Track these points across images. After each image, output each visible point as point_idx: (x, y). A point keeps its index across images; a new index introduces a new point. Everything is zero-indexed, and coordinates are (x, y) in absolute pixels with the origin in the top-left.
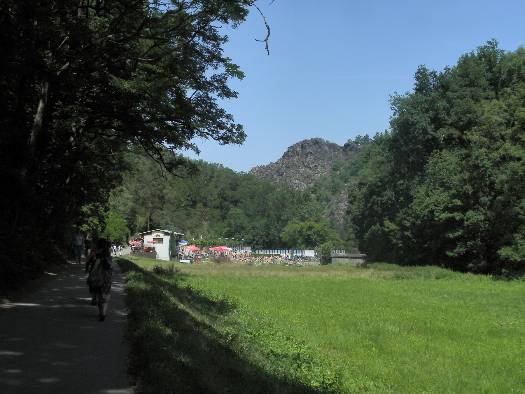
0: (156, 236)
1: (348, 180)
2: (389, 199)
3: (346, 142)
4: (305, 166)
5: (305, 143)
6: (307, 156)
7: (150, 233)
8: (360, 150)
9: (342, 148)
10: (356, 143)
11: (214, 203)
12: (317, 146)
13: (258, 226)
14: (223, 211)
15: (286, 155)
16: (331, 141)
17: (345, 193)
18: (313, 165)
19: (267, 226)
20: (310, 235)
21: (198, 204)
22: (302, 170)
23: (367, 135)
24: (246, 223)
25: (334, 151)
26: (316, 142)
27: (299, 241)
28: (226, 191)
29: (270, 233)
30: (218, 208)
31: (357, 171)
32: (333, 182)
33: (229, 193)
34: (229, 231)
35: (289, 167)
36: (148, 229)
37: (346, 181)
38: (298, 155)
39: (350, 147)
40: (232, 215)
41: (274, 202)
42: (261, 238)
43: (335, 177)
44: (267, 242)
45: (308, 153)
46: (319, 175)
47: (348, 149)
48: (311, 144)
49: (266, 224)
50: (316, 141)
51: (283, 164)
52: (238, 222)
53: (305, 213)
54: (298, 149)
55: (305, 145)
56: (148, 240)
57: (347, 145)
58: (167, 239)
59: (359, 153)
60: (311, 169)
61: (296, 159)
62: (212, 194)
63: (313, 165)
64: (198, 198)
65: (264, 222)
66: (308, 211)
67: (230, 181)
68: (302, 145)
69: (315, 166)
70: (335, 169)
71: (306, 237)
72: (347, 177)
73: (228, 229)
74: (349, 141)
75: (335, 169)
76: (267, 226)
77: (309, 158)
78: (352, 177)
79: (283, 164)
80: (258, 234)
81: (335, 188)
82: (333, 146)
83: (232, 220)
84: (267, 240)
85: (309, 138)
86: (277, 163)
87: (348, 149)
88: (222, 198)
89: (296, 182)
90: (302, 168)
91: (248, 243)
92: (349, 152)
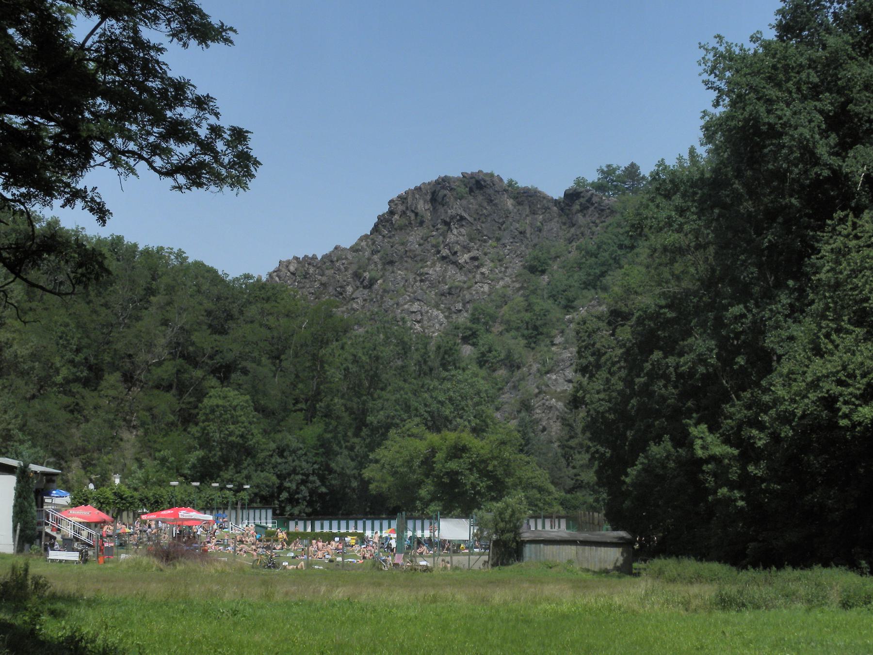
2: (701, 360)
3: (569, 184)
4: (444, 258)
5: (443, 188)
6: (450, 229)
8: (613, 212)
9: (556, 202)
10: (600, 187)
11: (158, 372)
12: (480, 198)
13: (294, 444)
14: (186, 398)
15: (383, 222)
16: (522, 183)
17: (566, 342)
18: (466, 256)
19: (322, 446)
20: (457, 473)
21: (106, 376)
22: (434, 270)
23: (633, 165)
24: (257, 438)
25: (534, 213)
26: (478, 184)
27: (423, 492)
28: (195, 337)
29: (333, 465)
30: (168, 388)
31: (603, 274)
32: (529, 308)
33: (204, 340)
34: (202, 460)
35: (391, 263)
37: (569, 307)
38: (421, 223)
39: (582, 200)
40: (213, 411)
41: (347, 369)
42: (304, 482)
43: (534, 292)
44: (322, 495)
45: (452, 218)
46: (486, 288)
47: (576, 207)
48: (463, 190)
49: (320, 437)
50: (478, 182)
52: (231, 434)
53: (442, 403)
54: (422, 206)
57: (572, 196)
59: (610, 220)
60: (461, 267)
61: (414, 238)
62: (150, 346)
63: (466, 256)
64: (107, 358)
65: (313, 431)
66: (451, 399)
67: (208, 305)
68: (434, 194)
69: (474, 259)
70: (535, 269)
71: (446, 480)
72: (569, 294)
73: (200, 453)
74: (579, 182)
75: (535, 269)
76: (322, 446)
77: (457, 235)
78: (590, 293)
79: (374, 252)
80: (294, 471)
81: (535, 328)
82: (528, 198)
83: (212, 427)
84: (323, 490)
85: (455, 173)
86: (355, 249)
87: (576, 207)
88: (183, 356)
89: (416, 307)
90: (433, 265)
91: (262, 500)
92: (580, 215)
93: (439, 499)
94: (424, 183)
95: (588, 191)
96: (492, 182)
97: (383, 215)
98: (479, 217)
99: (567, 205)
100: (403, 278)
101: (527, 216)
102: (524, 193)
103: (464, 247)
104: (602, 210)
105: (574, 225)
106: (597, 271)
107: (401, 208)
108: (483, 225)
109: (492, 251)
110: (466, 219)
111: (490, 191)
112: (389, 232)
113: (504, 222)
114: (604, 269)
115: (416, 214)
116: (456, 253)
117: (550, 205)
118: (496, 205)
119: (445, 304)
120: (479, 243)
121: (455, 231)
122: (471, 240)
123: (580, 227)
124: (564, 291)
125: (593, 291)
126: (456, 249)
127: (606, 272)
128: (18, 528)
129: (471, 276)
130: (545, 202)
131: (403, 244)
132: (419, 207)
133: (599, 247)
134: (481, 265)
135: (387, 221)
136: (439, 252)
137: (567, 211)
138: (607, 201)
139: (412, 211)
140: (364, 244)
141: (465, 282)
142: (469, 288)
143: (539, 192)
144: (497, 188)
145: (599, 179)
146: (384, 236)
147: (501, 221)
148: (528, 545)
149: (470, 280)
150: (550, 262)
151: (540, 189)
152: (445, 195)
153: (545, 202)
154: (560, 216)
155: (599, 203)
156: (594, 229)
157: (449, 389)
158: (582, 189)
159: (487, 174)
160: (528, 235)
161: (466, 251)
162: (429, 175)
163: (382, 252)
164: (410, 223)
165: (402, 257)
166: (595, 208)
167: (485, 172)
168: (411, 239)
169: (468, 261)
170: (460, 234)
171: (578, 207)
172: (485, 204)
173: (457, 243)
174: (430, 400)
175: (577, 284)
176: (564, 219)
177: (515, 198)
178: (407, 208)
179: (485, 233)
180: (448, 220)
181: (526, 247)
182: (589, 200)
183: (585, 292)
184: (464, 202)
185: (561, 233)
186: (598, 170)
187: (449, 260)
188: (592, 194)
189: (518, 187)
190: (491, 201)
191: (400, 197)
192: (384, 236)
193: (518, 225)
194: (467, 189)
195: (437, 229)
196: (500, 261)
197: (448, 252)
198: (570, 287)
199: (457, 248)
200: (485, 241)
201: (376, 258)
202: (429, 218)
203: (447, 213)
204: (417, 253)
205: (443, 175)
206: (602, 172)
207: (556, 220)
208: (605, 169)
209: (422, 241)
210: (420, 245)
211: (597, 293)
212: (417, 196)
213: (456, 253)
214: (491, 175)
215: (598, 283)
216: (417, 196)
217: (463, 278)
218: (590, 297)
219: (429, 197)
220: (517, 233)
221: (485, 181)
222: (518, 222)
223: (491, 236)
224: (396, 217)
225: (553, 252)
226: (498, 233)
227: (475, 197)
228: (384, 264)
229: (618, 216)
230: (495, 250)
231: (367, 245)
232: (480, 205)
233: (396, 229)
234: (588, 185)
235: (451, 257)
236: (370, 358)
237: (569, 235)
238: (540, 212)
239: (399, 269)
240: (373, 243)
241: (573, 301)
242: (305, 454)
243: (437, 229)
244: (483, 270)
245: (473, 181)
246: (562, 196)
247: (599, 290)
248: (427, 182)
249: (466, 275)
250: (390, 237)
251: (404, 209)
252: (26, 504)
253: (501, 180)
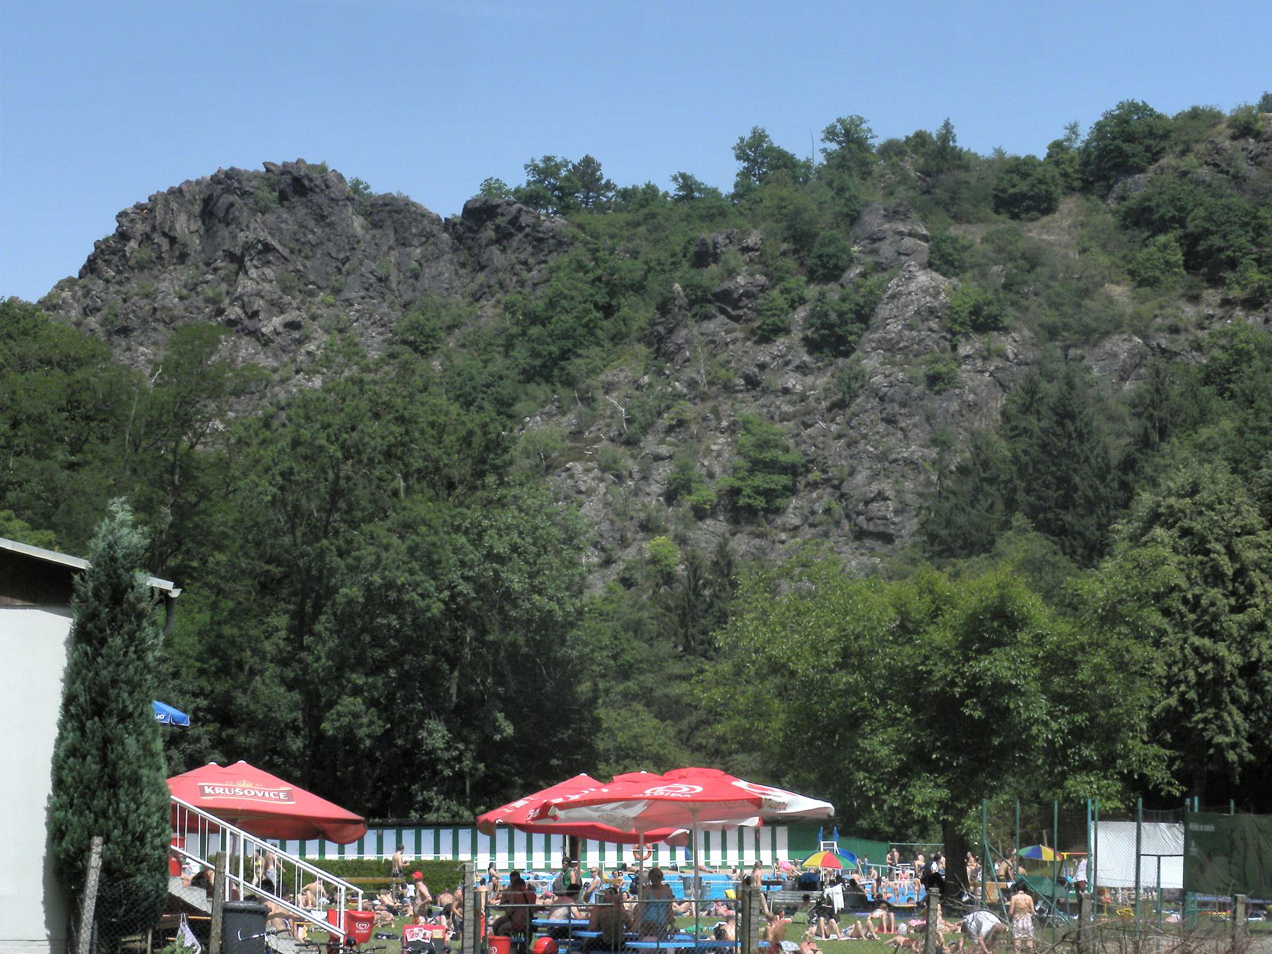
1: (518, 407)
3: (472, 191)
4: (231, 323)
5: (228, 190)
6: (242, 267)
8: (561, 244)
9: (449, 225)
10: (531, 198)
12: (301, 211)
16: (379, 187)
18: (277, 321)
20: (1002, 688)
23: (588, 161)
25: (404, 244)
26: (296, 185)
31: (565, 355)
35: (125, 331)
38: (183, 258)
39: (500, 221)
45: (247, 247)
51: (87, 312)
53: (500, 559)
54: (185, 226)
55: (226, 199)
57: (478, 213)
60: (265, 342)
61: (169, 285)
63: (277, 321)
66: (514, 548)
69: (293, 326)
72: (506, 389)
74: (490, 187)
77: (256, 280)
78: (540, 390)
79: (87, 312)
82: (393, 215)
85: (251, 163)
86: (49, 304)
92: (495, 249)
93: (933, 767)
94: (188, 182)
95: (509, 204)
96: (325, 181)
97: (106, 240)
98: (300, 247)
99: (470, 230)
100: (149, 361)
101: (391, 248)
102: (386, 205)
103: (272, 303)
104: (541, 240)
105: (483, 268)
106: (554, 349)
107: (141, 228)
108: (308, 263)
109: (324, 311)
110: (275, 249)
111: (319, 199)
112: (119, 272)
113: (348, 259)
114: (568, 344)
115: (173, 240)
116: (255, 314)
117: (435, 229)
118: (331, 225)
119: (236, 411)
120: (300, 297)
121: (253, 273)
122: (286, 290)
123: (497, 271)
124: (488, 386)
125: (546, 388)
126: (255, 308)
127: (569, 350)
128: (95, 861)
129: (286, 359)
130: (426, 222)
131: (147, 296)
132: (178, 226)
133: (552, 304)
134: (307, 338)
135: (114, 253)
136: (220, 312)
137: (470, 242)
138: (547, 224)
139: (165, 234)
140: (66, 294)
141: (275, 371)
142: (283, 381)
143: (413, 204)
144: (334, 193)
145: (529, 183)
146: (107, 281)
147: (342, 256)
149: (285, 365)
150: (443, 334)
151: (413, 199)
152: (232, 205)
153: (426, 222)
154: (455, 250)
155: (535, 227)
156: (525, 275)
157: (508, 528)
158: (497, 201)
159: (313, 167)
160: (394, 286)
161: (275, 310)
162: (200, 167)
163: (105, 311)
164: (160, 258)
165: (145, 321)
166: (527, 236)
167: (309, 162)
168: (164, 286)
169: (280, 329)
170: (264, 279)
171: (491, 234)
172: (311, 223)
173: (259, 294)
174: (474, 555)
175: (513, 374)
176: (463, 256)
177: (367, 215)
178: (154, 228)
179: (312, 278)
180: (238, 252)
181: (391, 306)
182: (514, 221)
183: (531, 387)
184: (270, 218)
185: (457, 283)
186: (526, 167)
188: (520, 210)
189: (370, 195)
190: (323, 217)
191: (140, 207)
192: (107, 281)
193: (374, 266)
194: (276, 194)
195: (216, 270)
196: (340, 331)
197: (239, 311)
198: (501, 378)
199: (259, 304)
200: (311, 294)
201: (93, 321)
202: (199, 248)
203: (235, 238)
204: (176, 312)
205: (226, 167)
206: (535, 169)
207: (448, 256)
208: (541, 165)
209: (185, 292)
210: (181, 298)
211: (554, 392)
212: (174, 206)
213: (255, 314)
214: (322, 169)
215: (556, 372)
216: (174, 206)
217: (272, 363)
218: (543, 398)
219: (197, 209)
220: (373, 280)
221: (311, 180)
222: (374, 259)
223: (323, 283)
224: (133, 244)
225: (446, 319)
226: (335, 280)
227: (291, 210)
228: (109, 334)
229: (579, 251)
230: (332, 311)
231: (73, 297)
232: (302, 226)
233: (132, 269)
234: (507, 193)
235: (246, 322)
236: (343, 447)
237: (473, 286)
238: (415, 242)
239: (141, 344)
240: (87, 294)
241: (510, 405)
242: (176, 675)
243: (216, 270)
244: (312, 347)
245: (288, 179)
246: (459, 212)
247: (559, 386)
248: (193, 179)
249: (275, 356)
250: (120, 283)
251: (148, 229)
252: (131, 742)
253: (341, 178)
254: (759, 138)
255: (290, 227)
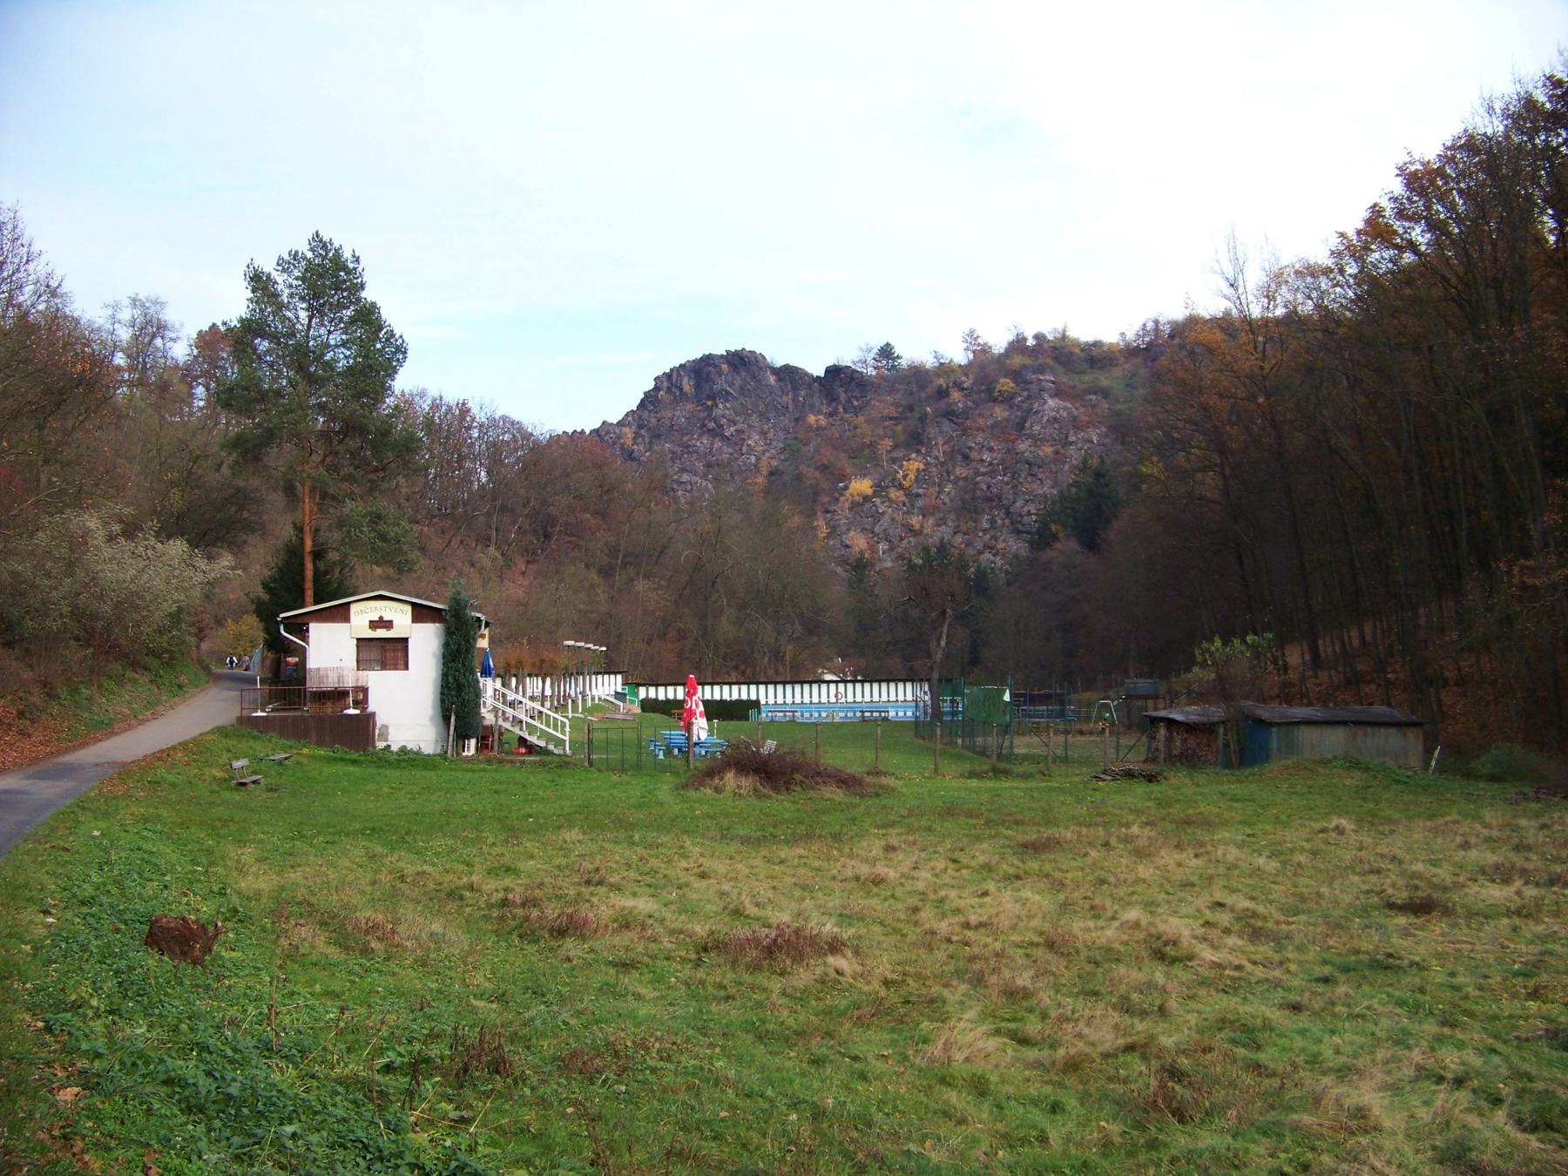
0: (374, 625)
7: (342, 614)
12: (743, 374)
15: (649, 400)
22: (703, 443)
23: (888, 345)
26: (743, 362)
35: (658, 436)
36: (309, 594)
50: (742, 359)
56: (329, 650)
58: (425, 642)
82: (789, 374)
85: (720, 350)
86: (621, 423)
89: (685, 477)
111: (754, 368)
148: (1274, 730)
187: (717, 433)
254: (972, 332)
255: (738, 381)
